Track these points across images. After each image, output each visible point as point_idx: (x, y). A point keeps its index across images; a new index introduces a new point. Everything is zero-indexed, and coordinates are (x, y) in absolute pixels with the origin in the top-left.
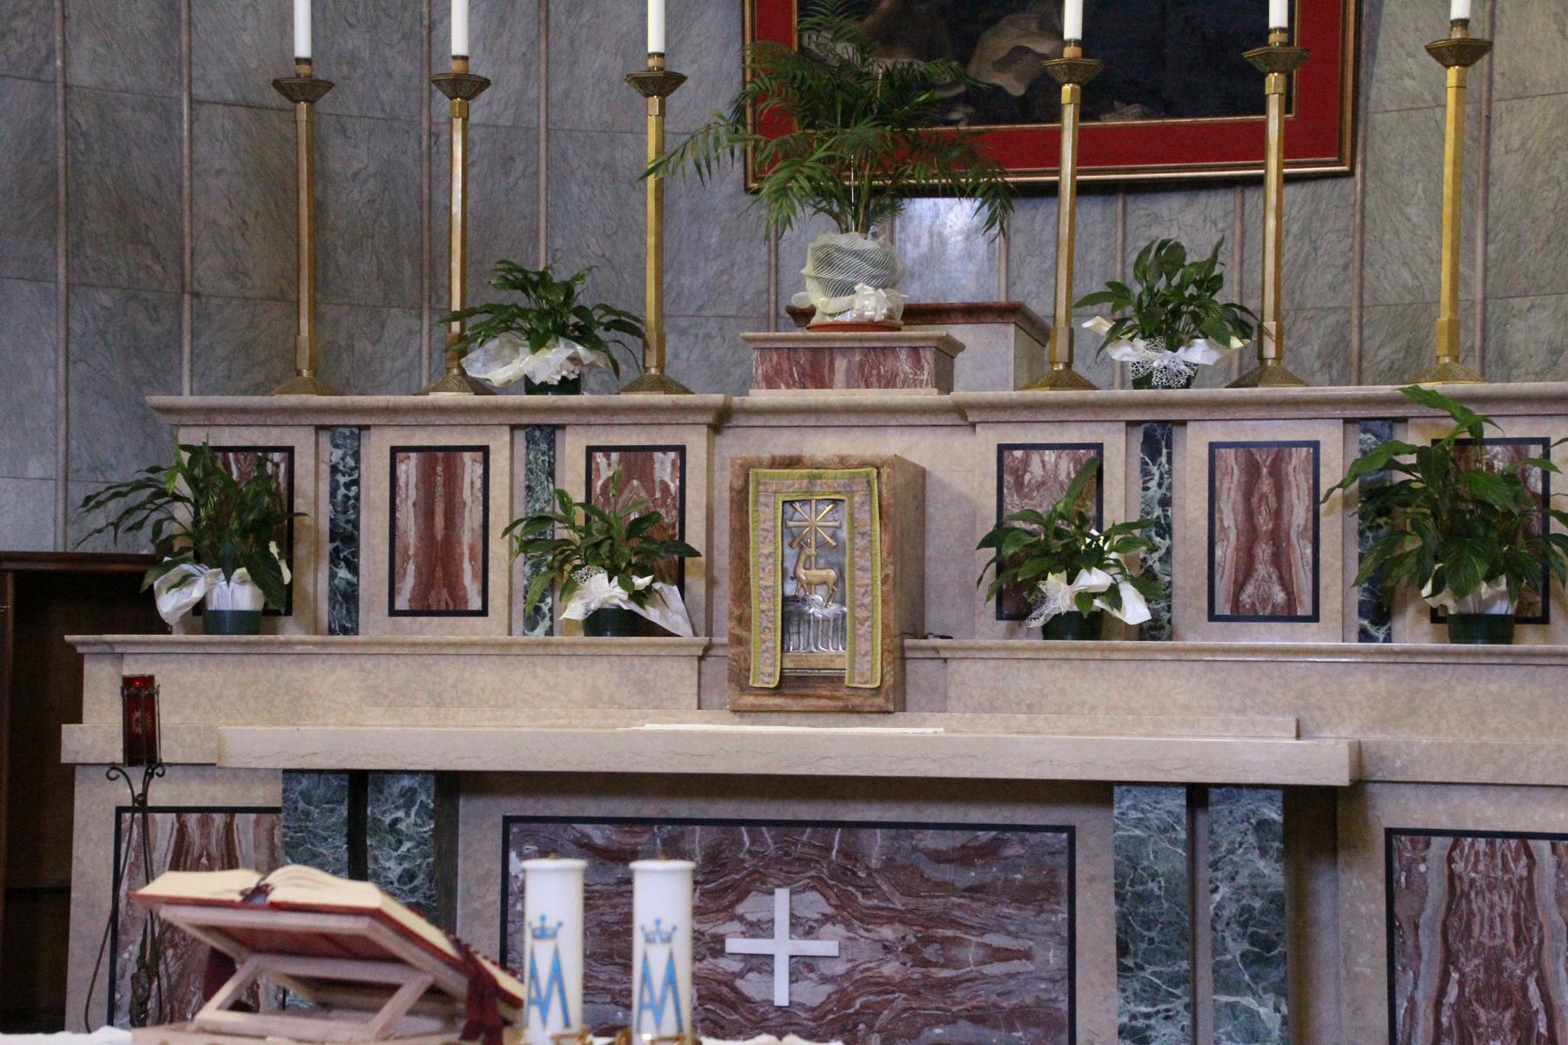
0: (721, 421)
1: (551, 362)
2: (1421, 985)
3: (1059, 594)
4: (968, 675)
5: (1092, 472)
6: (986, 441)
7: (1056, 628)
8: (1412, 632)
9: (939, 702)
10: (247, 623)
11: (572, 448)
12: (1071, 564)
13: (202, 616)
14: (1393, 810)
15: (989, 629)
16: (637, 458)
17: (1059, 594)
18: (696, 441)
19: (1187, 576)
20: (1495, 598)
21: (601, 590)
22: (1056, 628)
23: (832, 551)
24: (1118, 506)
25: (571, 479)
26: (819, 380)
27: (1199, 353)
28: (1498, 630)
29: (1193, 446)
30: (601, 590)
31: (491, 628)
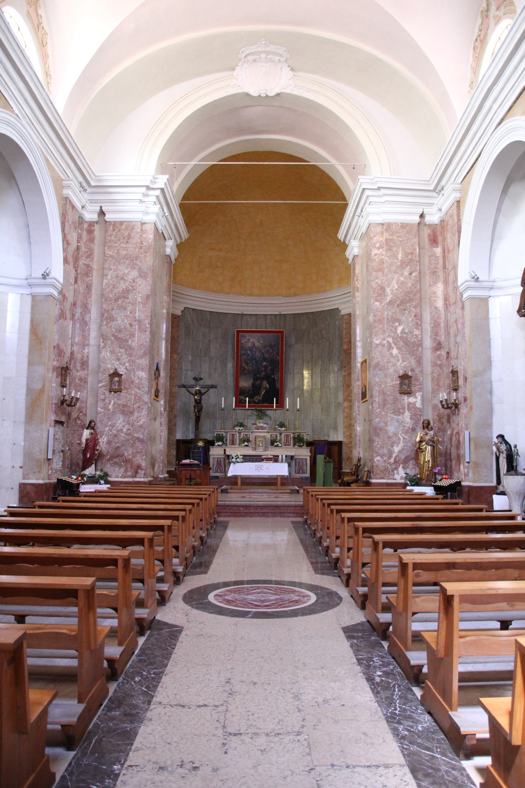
0: (252, 432)
1: (241, 429)
2: (297, 467)
3: (276, 444)
4: (269, 449)
5: (277, 436)
6: (270, 434)
7: (276, 446)
8: (296, 446)
9: (268, 451)
10: (221, 445)
11: (242, 434)
12: (277, 442)
13: (219, 445)
14: (296, 457)
15: (270, 446)
16: (246, 435)
17: (276, 444)
18: (250, 434)
19: (283, 442)
20: (302, 444)
21: (246, 443)
22: (276, 446)
23: (261, 441)
24: (278, 438)
25: (242, 436)
26: (258, 429)
27: (283, 429)
28: (301, 446)
29: (283, 435)
30: (246, 443)
31: (237, 446)
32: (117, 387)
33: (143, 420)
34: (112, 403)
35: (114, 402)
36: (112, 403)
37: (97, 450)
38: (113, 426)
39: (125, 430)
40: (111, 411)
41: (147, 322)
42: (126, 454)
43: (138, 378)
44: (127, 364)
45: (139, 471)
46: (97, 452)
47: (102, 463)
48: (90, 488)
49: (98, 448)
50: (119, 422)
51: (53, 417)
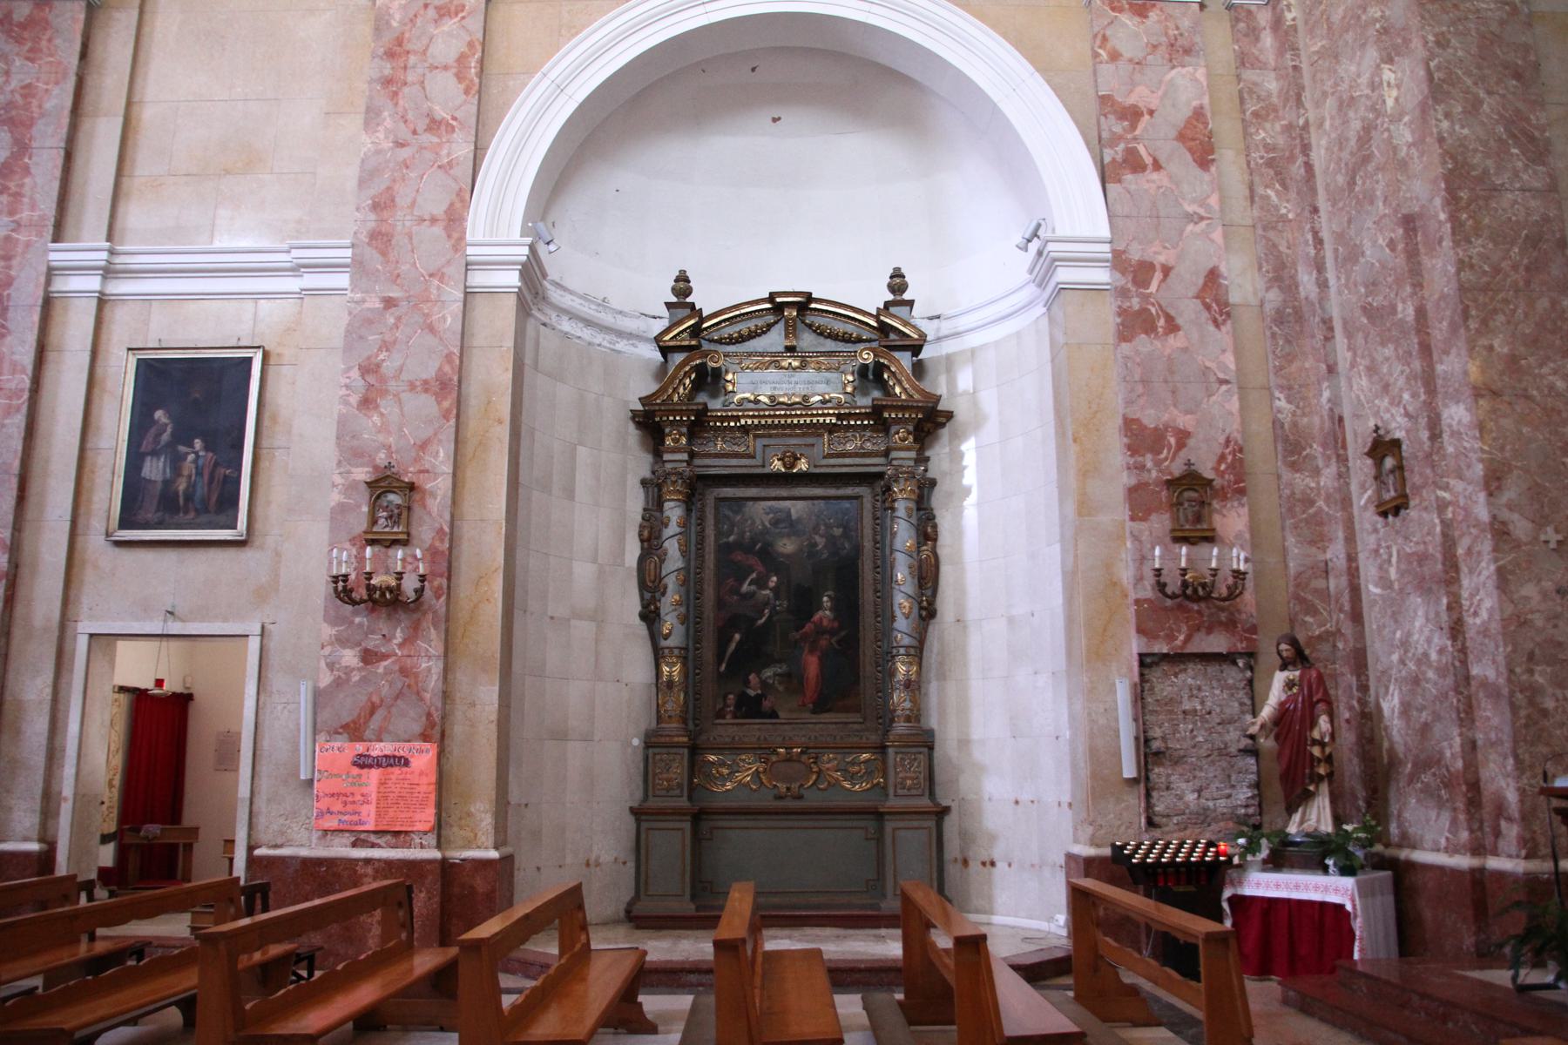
32: (1393, 493)
33: (1488, 604)
34: (1394, 560)
35: (1398, 552)
36: (1394, 560)
37: (1314, 742)
38: (1405, 644)
39: (1434, 656)
40: (1396, 586)
41: (1438, 202)
42: (1448, 754)
43: (1453, 434)
44: (1406, 396)
45: (1503, 824)
46: (1316, 751)
47: (1398, 789)
48: (1278, 886)
49: (1316, 734)
50: (1417, 624)
51: (1134, 645)
